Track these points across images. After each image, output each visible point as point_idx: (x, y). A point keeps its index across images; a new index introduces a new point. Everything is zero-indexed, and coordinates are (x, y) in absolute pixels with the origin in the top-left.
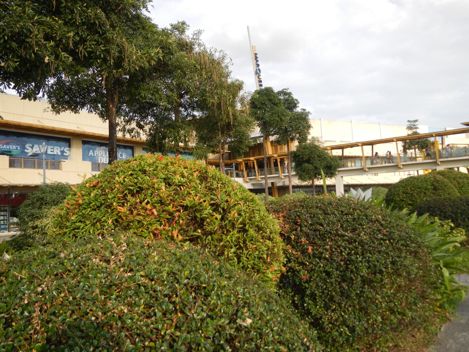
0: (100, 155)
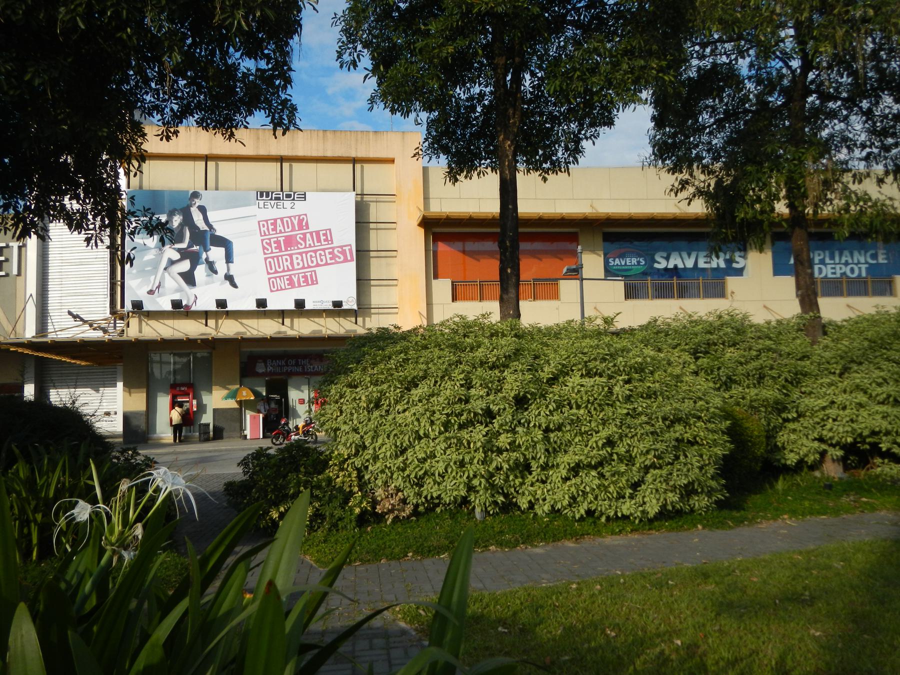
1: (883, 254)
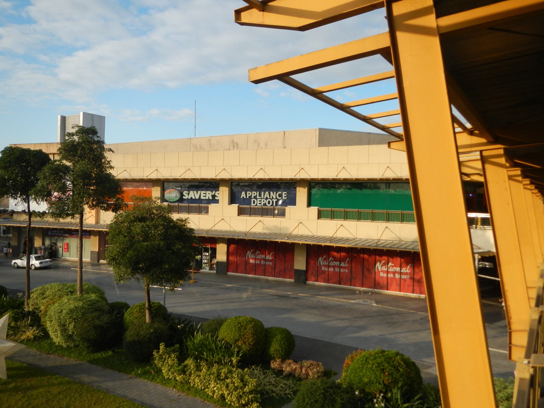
0: (253, 197)
1: (285, 194)
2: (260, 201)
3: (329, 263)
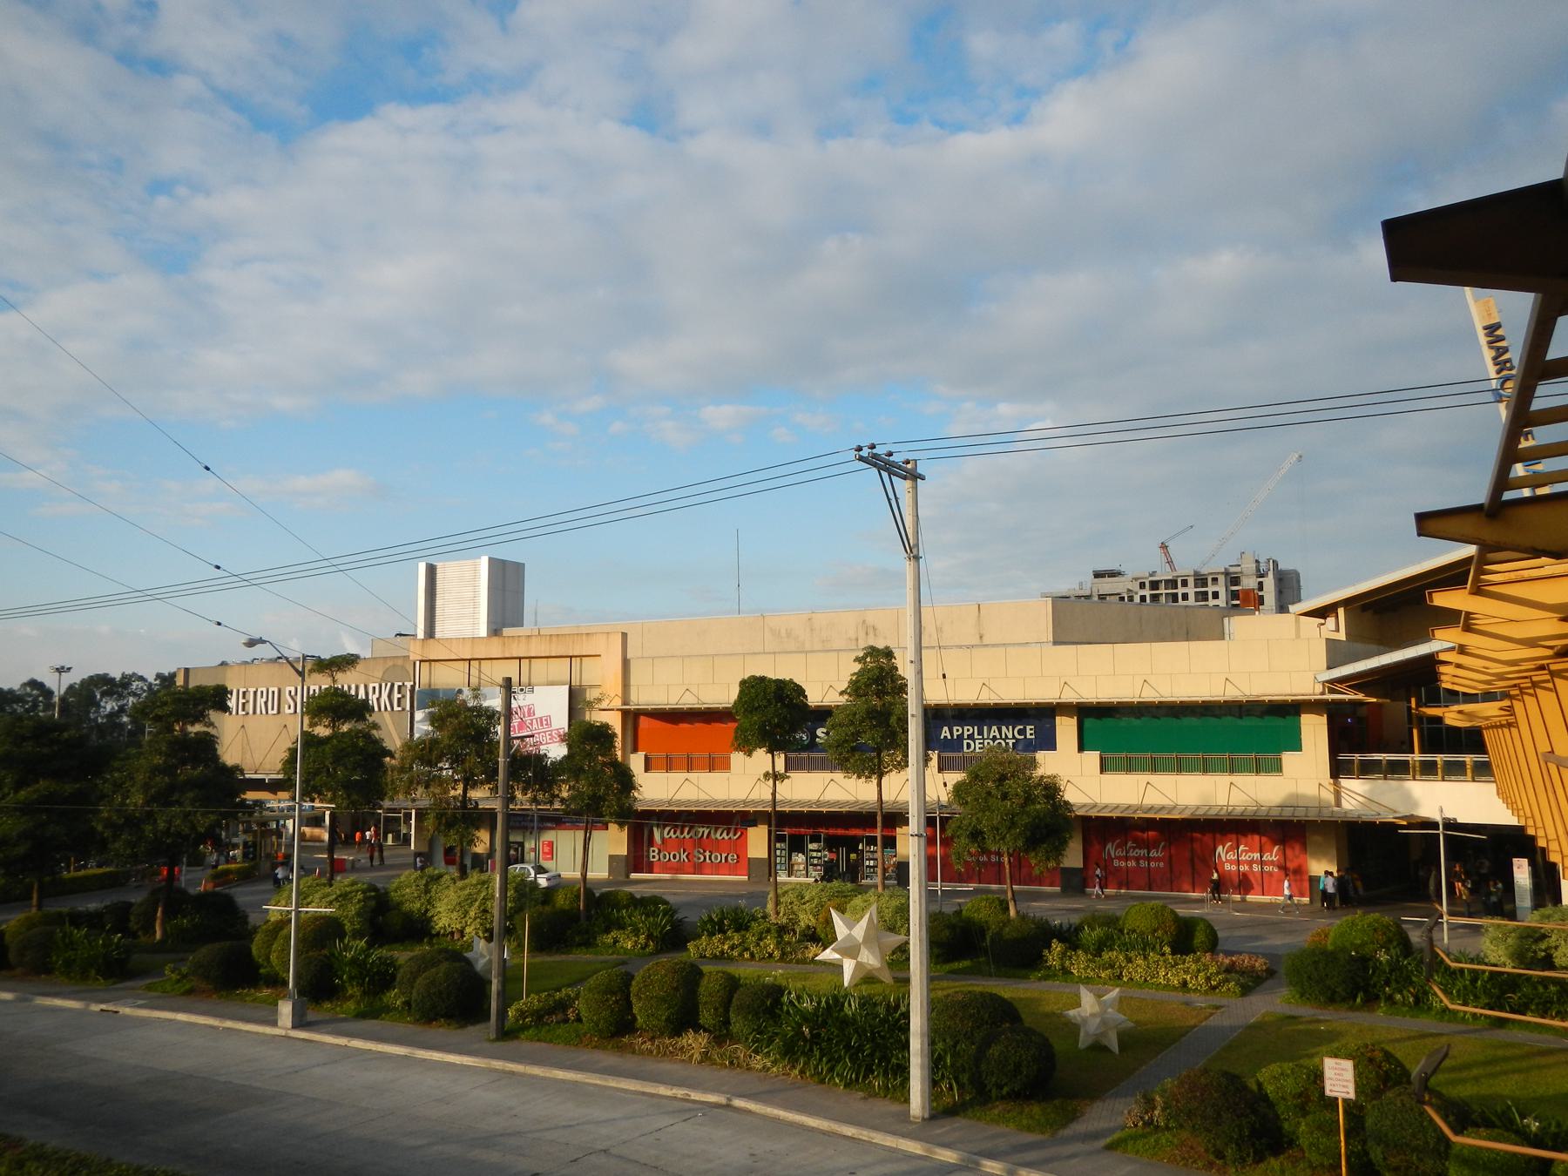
0: (966, 737)
1: (1031, 729)
2: (980, 743)
3: (1127, 853)
